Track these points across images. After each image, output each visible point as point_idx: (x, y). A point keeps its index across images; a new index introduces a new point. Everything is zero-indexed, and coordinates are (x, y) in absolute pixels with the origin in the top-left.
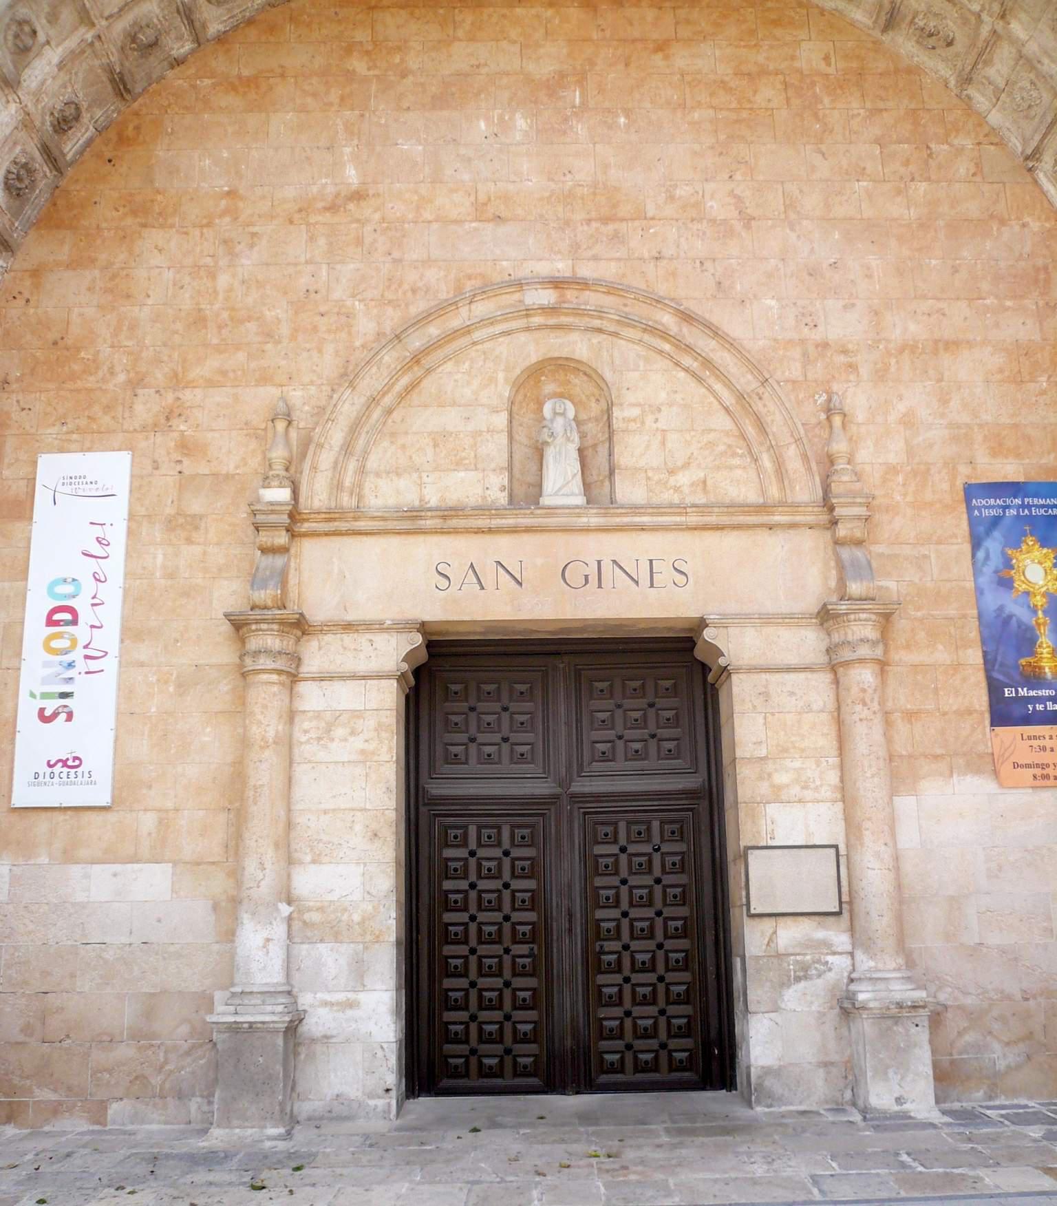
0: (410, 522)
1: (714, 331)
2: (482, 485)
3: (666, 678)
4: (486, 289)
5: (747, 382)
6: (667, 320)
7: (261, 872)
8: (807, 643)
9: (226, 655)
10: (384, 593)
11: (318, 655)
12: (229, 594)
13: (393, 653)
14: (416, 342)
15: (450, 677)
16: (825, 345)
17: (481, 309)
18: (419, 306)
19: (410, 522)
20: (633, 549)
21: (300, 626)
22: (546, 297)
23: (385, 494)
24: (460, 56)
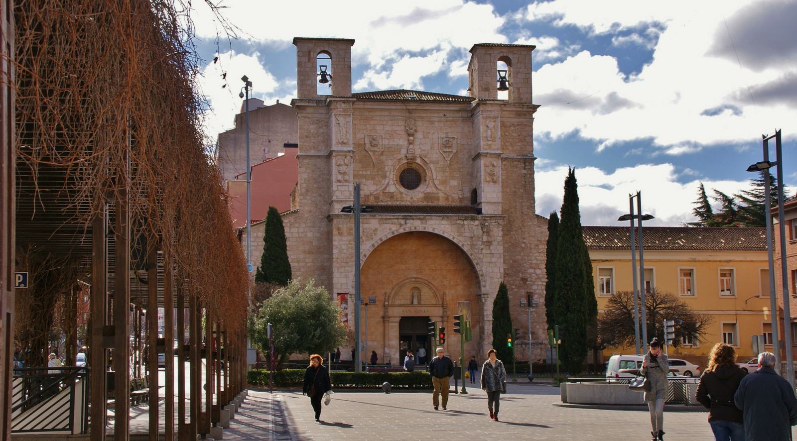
0: (400, 306)
1: (432, 284)
2: (409, 302)
3: (425, 321)
4: (407, 279)
5: (435, 290)
6: (427, 282)
7: (387, 343)
8: (440, 319)
9: (382, 320)
10: (397, 313)
11: (391, 320)
12: (381, 314)
13: (398, 319)
14: (400, 285)
15: (405, 321)
16: (444, 285)
17: (407, 281)
18: (400, 280)
19: (400, 306)
20: (423, 309)
21: (389, 317)
22: (414, 280)
23: (397, 302)
24: (405, 247)
